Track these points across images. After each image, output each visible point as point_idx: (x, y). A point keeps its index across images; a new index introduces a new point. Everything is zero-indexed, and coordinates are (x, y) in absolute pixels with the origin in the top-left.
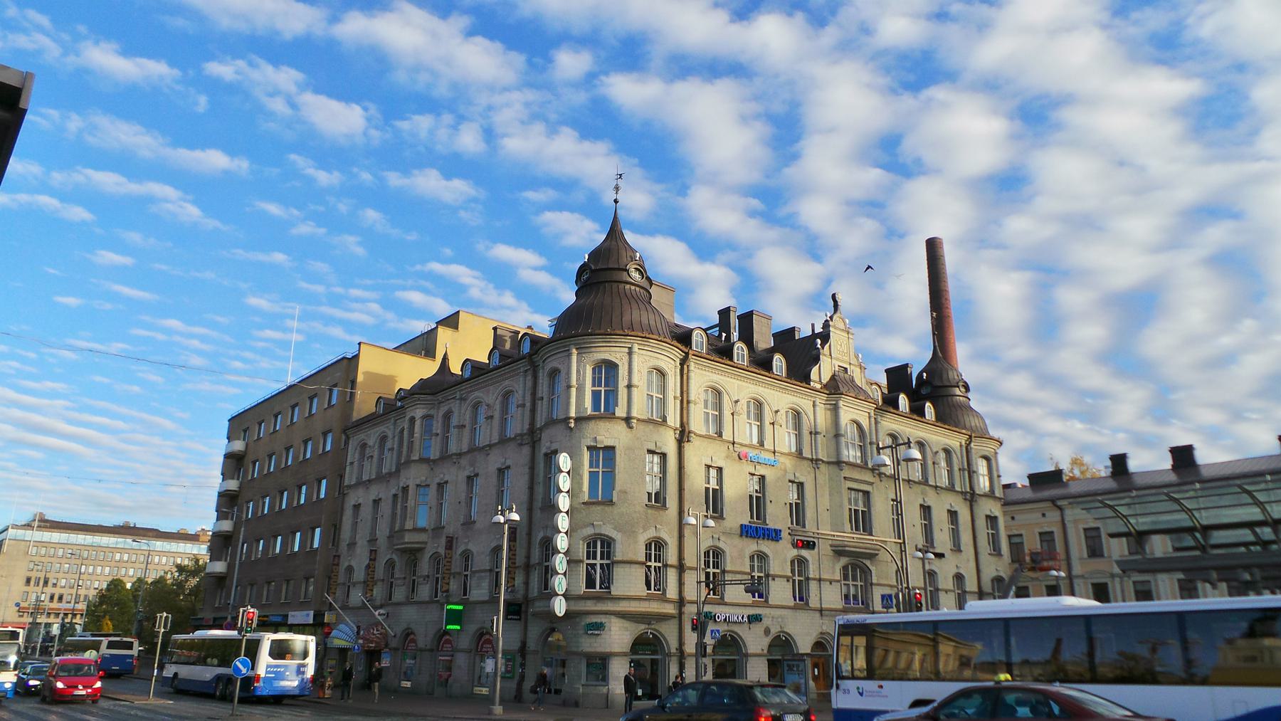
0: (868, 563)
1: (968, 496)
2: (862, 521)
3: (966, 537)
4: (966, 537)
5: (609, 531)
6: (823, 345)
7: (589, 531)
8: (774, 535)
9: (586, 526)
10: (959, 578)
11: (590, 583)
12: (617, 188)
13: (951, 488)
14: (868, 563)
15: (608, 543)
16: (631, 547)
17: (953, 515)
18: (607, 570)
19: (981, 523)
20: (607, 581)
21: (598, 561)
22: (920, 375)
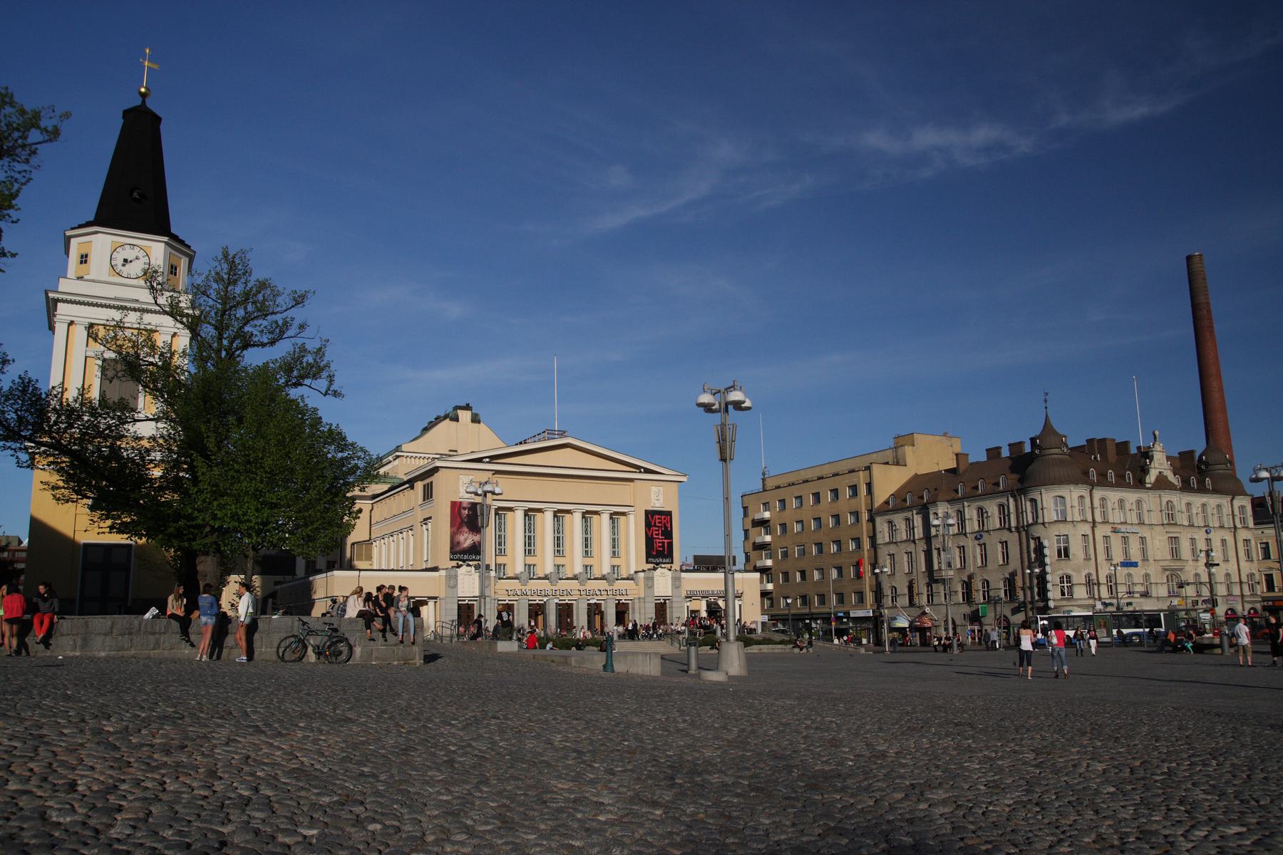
0: (1179, 573)
1: (1233, 530)
2: (1175, 553)
3: (1232, 553)
4: (1232, 553)
5: (1069, 572)
6: (1150, 462)
7: (1060, 573)
8: (1135, 565)
9: (1059, 570)
10: (1228, 575)
11: (1063, 594)
12: (1046, 401)
13: (1222, 527)
14: (1179, 573)
15: (1069, 577)
16: (1079, 578)
17: (1224, 542)
18: (1070, 588)
19: (1240, 544)
20: (1070, 593)
21: (1065, 585)
22: (1200, 457)
